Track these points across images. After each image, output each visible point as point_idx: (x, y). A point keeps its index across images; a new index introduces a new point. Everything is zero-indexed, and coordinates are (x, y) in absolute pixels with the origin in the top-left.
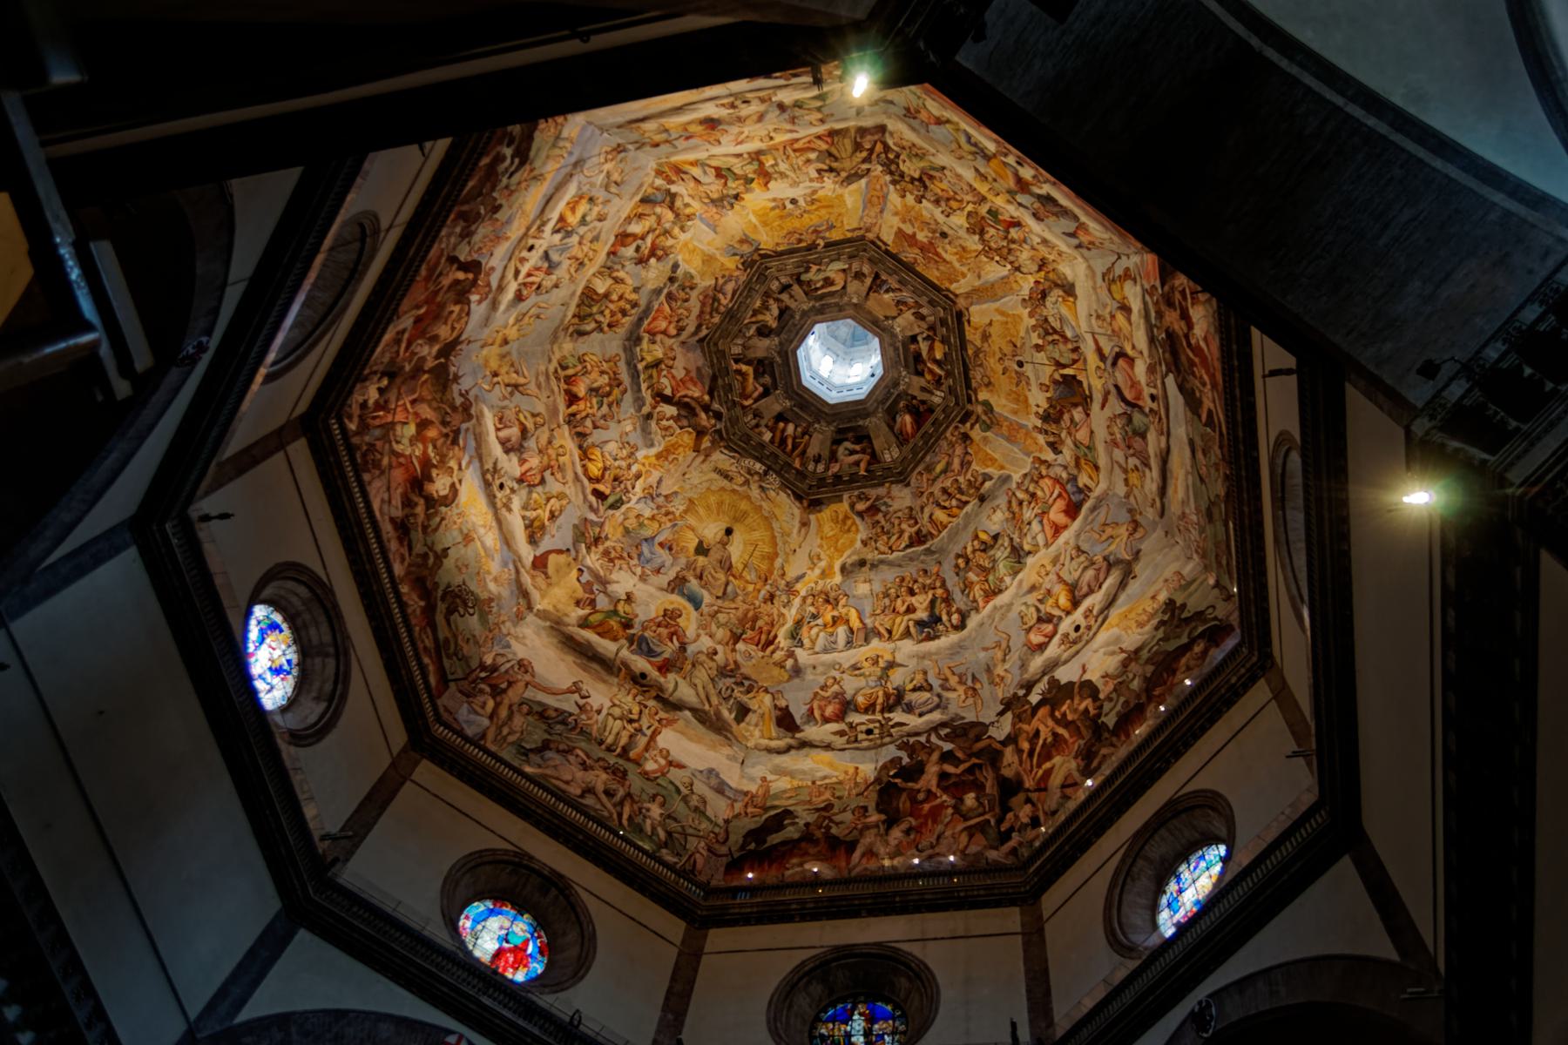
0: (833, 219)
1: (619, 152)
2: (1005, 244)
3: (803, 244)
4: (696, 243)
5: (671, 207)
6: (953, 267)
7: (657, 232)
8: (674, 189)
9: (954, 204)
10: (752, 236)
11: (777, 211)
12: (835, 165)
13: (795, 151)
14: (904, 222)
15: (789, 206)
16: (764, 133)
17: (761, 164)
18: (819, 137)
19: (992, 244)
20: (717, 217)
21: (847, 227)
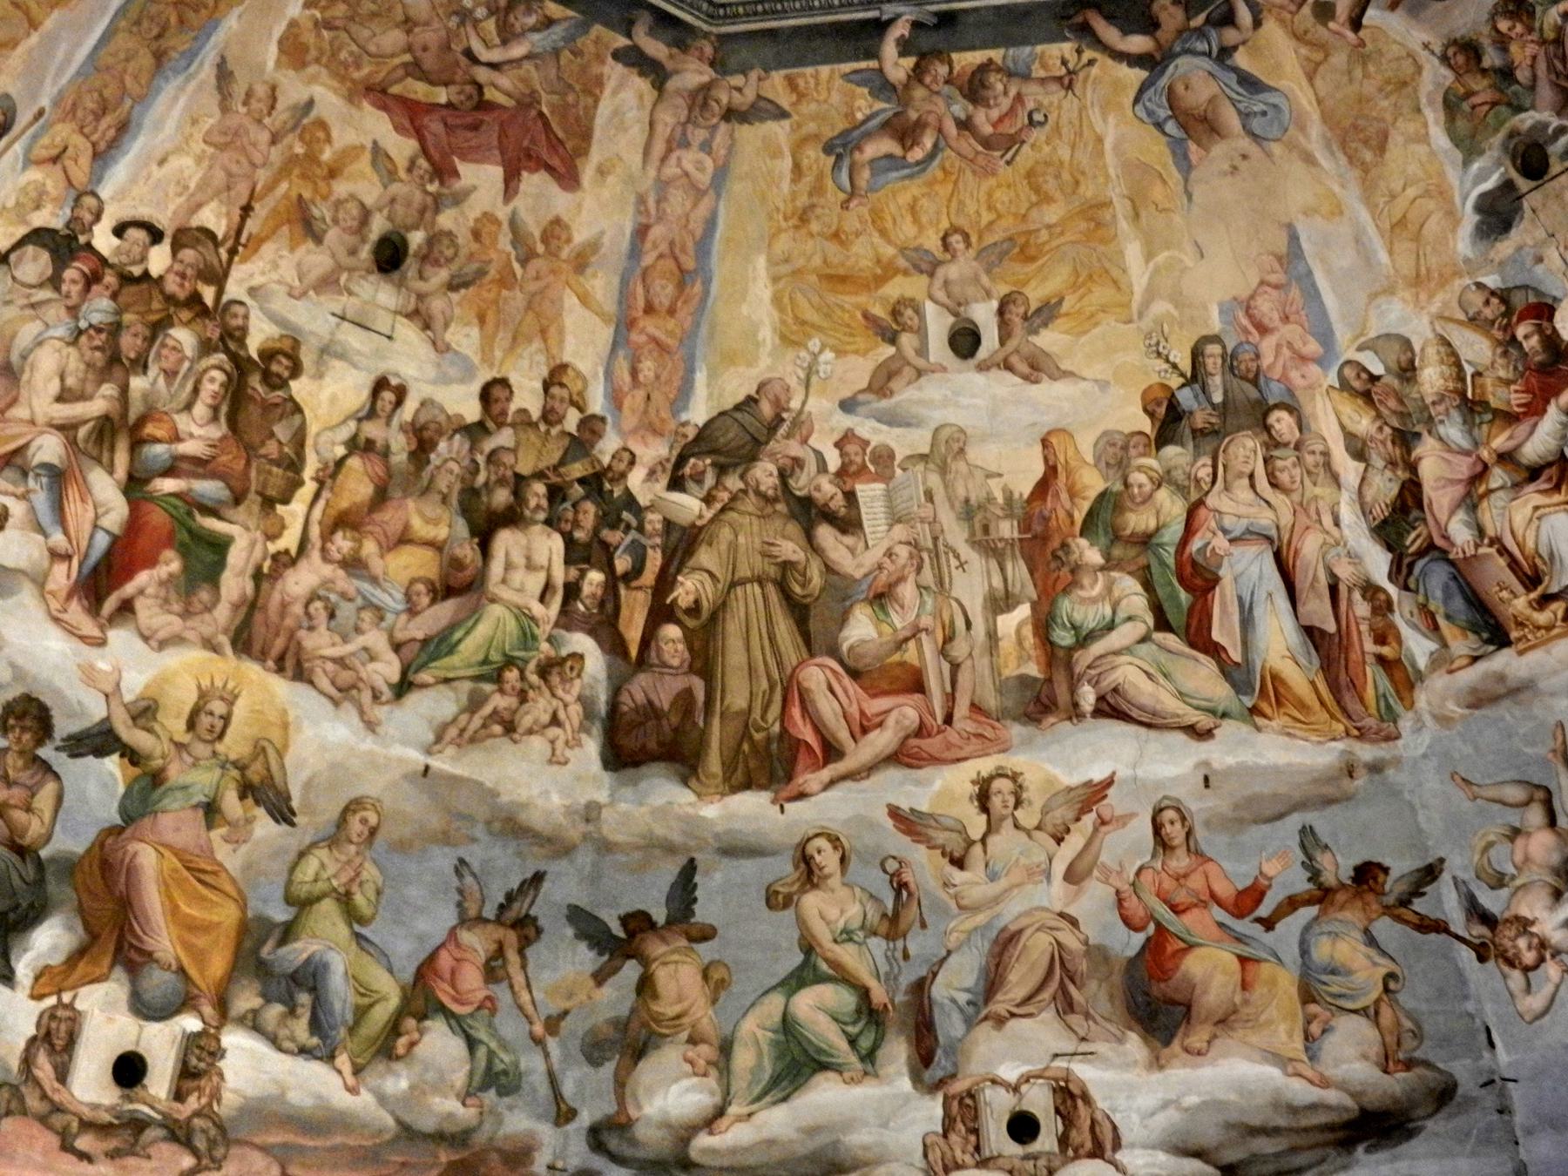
0: (834, 196)
1: (1488, 919)
2: (138, 383)
3: (967, 60)
4: (1383, 257)
5: (1410, 498)
6: (339, 71)
7: (1501, 441)
8: (1378, 564)
9: (357, 485)
10: (1155, 149)
11: (1035, 294)
12: (790, 549)
13: (917, 685)
14: (555, 230)
15: (984, 314)
16: (1005, 842)
17: (1043, 624)
18: (831, 752)
19: (184, 337)
20: (1266, 307)
21: (779, 131)
